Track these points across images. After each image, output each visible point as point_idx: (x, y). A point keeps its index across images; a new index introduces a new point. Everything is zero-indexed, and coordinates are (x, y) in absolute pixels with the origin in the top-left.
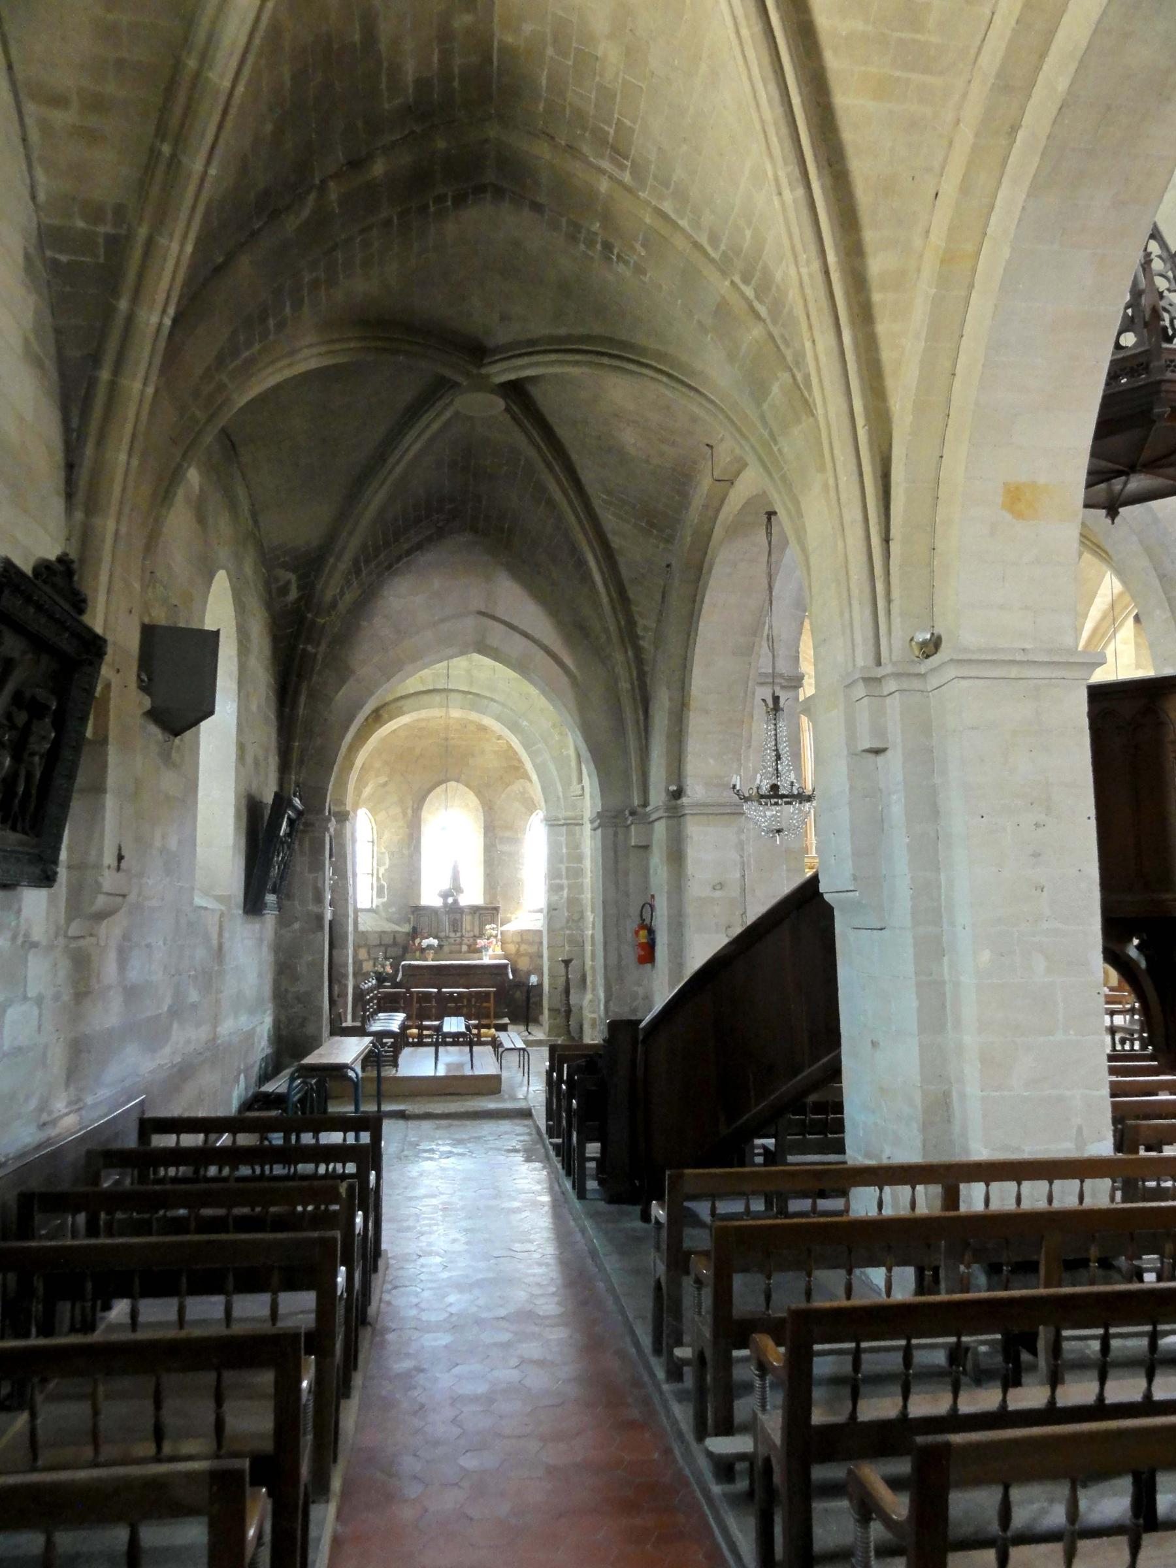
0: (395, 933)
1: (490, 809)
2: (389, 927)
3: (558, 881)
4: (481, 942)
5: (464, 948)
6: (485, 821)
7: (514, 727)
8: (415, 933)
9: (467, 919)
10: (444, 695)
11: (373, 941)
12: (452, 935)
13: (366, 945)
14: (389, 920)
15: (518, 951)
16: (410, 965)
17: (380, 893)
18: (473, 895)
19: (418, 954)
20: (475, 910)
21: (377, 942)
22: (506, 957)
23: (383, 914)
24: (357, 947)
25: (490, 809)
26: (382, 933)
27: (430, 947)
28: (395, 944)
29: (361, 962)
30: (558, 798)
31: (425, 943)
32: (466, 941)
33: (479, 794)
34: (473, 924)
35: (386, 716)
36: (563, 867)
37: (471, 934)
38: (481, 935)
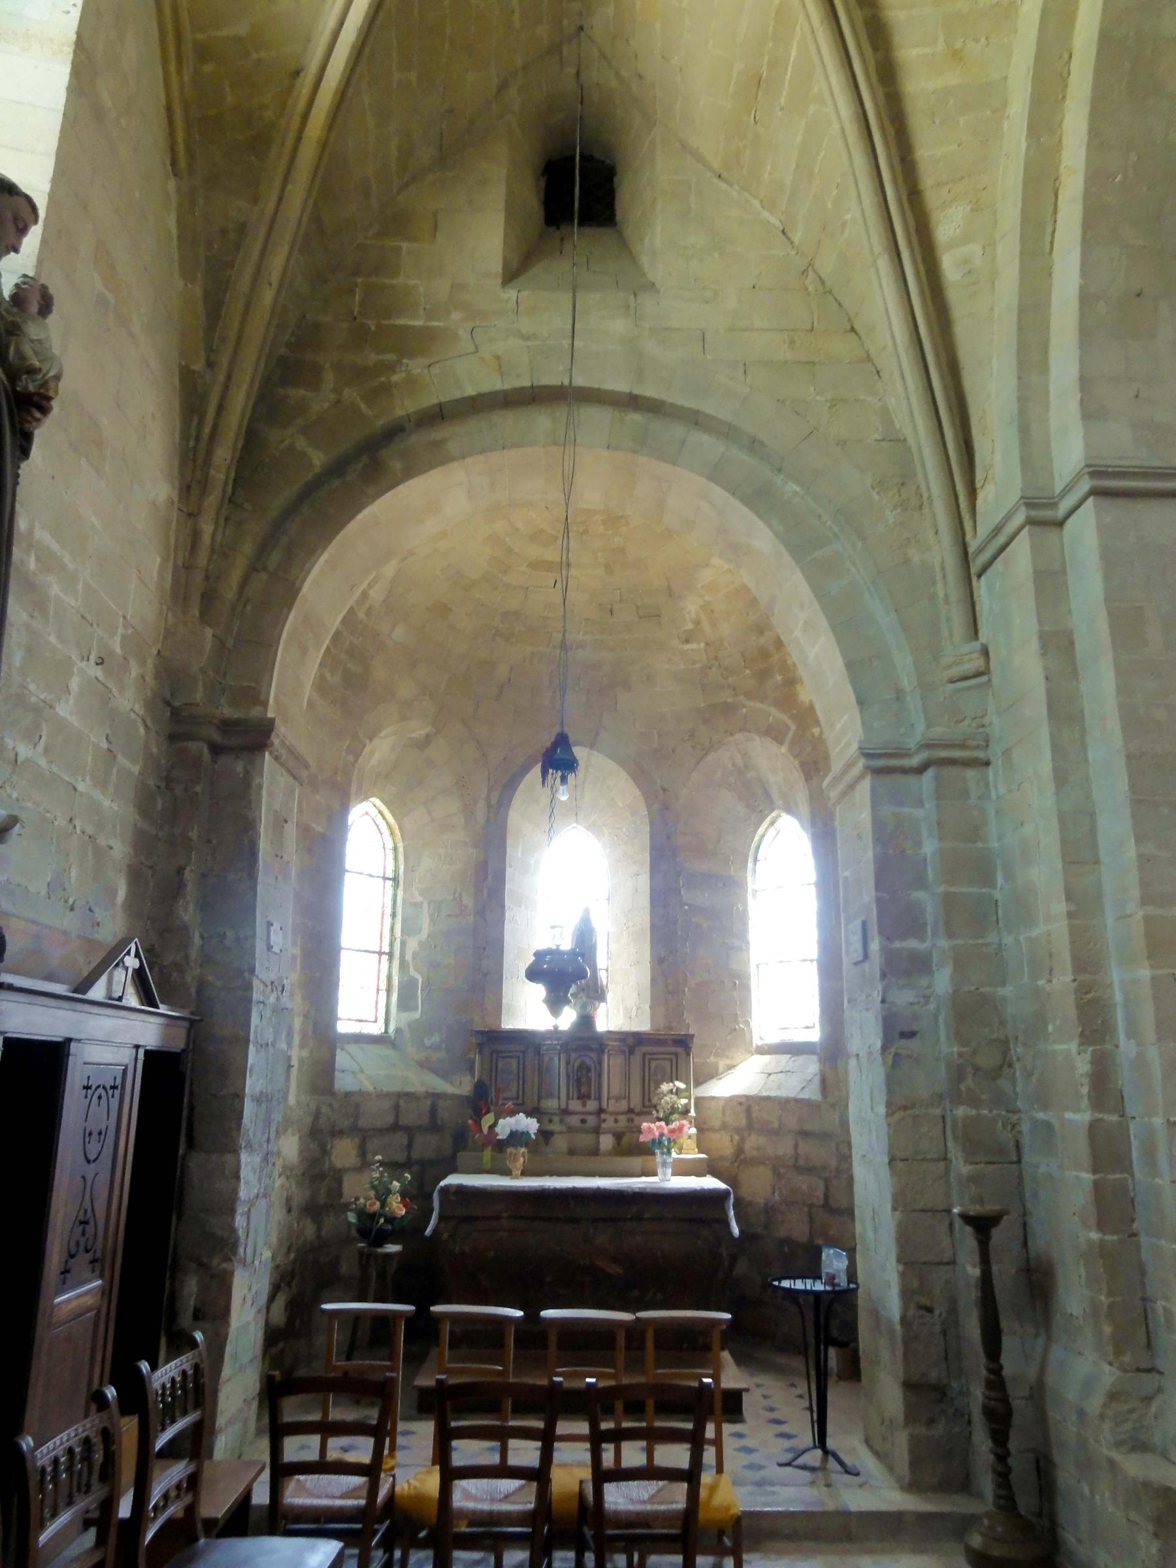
0: (436, 1096)
1: (666, 807)
3: (912, 944)
4: (651, 1129)
5: (606, 1142)
6: (653, 837)
7: (759, 499)
8: (480, 1101)
9: (612, 1065)
10: (561, 412)
11: (377, 1115)
12: (575, 1105)
13: (354, 1129)
14: (424, 1064)
15: (740, 1151)
16: (461, 1190)
17: (405, 1003)
18: (620, 1011)
19: (488, 1154)
20: (631, 1042)
21: (390, 1119)
23: (411, 1050)
24: (319, 1135)
25: (666, 807)
26: (400, 1099)
27: (516, 1138)
28: (434, 1126)
29: (337, 1176)
30: (899, 695)
31: (506, 1126)
32: (609, 1123)
33: (639, 774)
34: (627, 1077)
35: (397, 465)
36: (928, 901)
38: (648, 1108)
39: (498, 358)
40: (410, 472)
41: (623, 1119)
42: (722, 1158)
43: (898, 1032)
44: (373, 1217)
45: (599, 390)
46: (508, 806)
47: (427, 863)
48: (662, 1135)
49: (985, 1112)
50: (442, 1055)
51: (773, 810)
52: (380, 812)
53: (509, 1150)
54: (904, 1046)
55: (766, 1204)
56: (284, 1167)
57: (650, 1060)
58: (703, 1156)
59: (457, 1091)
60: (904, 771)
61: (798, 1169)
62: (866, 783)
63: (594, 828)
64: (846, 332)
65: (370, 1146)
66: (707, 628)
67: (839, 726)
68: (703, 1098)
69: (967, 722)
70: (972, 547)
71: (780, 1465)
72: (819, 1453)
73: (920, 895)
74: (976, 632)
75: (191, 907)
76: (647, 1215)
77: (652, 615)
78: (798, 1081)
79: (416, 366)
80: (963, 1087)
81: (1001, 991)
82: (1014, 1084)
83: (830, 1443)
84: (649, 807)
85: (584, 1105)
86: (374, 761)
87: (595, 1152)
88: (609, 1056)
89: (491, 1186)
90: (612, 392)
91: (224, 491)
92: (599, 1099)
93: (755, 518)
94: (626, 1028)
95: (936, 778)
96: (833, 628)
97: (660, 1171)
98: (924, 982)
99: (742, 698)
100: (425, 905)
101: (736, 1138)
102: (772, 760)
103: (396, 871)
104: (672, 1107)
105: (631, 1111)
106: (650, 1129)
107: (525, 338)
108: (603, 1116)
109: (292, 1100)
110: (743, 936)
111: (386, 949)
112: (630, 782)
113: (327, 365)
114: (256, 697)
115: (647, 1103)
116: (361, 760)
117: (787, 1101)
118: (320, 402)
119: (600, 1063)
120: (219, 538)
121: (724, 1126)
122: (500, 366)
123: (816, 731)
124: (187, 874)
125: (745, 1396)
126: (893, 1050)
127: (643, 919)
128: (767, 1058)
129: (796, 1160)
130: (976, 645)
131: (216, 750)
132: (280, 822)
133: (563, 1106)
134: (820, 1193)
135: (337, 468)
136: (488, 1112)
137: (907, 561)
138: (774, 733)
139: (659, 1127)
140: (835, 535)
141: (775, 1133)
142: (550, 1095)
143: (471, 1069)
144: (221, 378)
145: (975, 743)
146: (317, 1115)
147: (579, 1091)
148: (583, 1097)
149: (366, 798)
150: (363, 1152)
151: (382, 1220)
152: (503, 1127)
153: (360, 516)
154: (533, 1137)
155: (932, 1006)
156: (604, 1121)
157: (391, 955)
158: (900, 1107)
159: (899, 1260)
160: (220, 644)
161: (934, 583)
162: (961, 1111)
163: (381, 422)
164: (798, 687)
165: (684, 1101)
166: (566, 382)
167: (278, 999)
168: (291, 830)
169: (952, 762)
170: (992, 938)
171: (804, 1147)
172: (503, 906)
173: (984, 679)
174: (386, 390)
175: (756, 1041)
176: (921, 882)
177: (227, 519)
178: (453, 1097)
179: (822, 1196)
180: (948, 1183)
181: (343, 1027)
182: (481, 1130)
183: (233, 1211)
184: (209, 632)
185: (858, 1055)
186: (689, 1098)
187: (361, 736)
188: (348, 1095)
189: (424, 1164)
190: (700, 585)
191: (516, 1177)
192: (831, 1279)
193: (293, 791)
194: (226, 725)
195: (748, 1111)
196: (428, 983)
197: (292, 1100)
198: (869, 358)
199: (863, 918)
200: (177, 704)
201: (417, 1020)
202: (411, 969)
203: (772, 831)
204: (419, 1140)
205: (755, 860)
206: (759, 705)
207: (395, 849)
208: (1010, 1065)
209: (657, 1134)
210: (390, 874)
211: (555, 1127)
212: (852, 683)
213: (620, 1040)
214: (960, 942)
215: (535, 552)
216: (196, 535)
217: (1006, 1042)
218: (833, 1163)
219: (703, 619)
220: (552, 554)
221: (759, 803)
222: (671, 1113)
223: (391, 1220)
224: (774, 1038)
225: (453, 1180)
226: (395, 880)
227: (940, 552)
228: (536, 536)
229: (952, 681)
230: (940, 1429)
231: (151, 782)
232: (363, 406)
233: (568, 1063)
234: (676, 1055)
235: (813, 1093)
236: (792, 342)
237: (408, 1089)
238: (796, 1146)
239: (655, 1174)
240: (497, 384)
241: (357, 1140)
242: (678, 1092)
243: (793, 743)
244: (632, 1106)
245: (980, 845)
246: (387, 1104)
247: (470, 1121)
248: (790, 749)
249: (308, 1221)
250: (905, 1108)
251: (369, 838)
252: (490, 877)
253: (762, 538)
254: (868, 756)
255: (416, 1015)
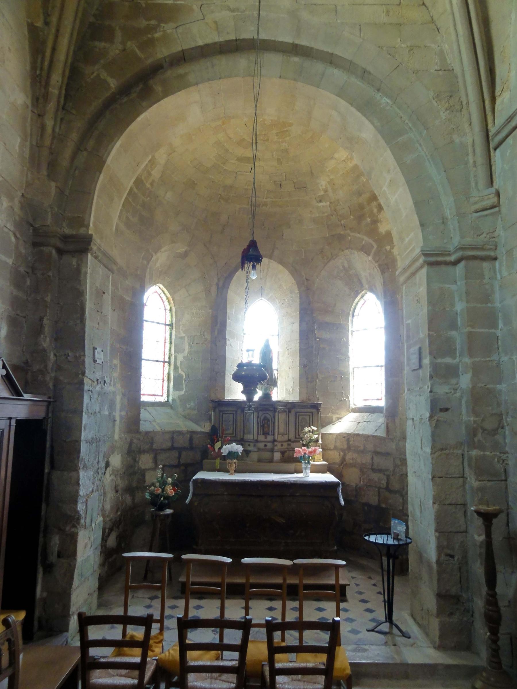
0: (193, 433)
1: (308, 289)
2: (185, 426)
3: (448, 360)
4: (300, 451)
5: (277, 456)
6: (301, 304)
7: (366, 107)
8: (214, 435)
9: (280, 418)
12: (262, 438)
13: (151, 450)
15: (343, 460)
16: (204, 481)
17: (177, 386)
18: (284, 390)
19: (218, 461)
20: (289, 407)
21: (169, 444)
22: (329, 469)
23: (180, 410)
24: (132, 453)
26: (174, 434)
27: (232, 455)
28: (191, 447)
29: (143, 473)
30: (444, 221)
31: (226, 449)
32: (278, 447)
33: (295, 272)
34: (287, 423)
35: (159, 89)
37: (286, 438)
39: (216, 22)
40: (166, 94)
41: (285, 444)
42: (334, 463)
43: (439, 408)
44: (158, 496)
45: (274, 41)
46: (228, 288)
47: (187, 317)
48: (305, 454)
49: (488, 453)
50: (195, 412)
51: (363, 290)
52: (163, 291)
53: (228, 461)
54: (443, 416)
55: (356, 486)
56: (113, 471)
57: (299, 415)
58: (325, 463)
59: (203, 430)
60: (446, 263)
61: (374, 470)
62: (424, 270)
63: (272, 300)
64: (419, 5)
65: (159, 457)
66: (330, 193)
67: (407, 240)
68: (325, 434)
69: (484, 235)
70: (492, 130)
71: (368, 631)
72: (388, 624)
73: (454, 333)
74: (492, 182)
75: (48, 339)
76: (298, 494)
77: (301, 187)
78: (375, 426)
79: (168, 28)
80: (476, 439)
81: (498, 387)
82: (505, 438)
83: (394, 618)
84: (299, 289)
85: (266, 438)
86: (158, 265)
87: (271, 461)
88: (279, 413)
89: (219, 479)
90: (282, 43)
91: (58, 101)
92: (274, 435)
93: (364, 119)
94: (287, 399)
95: (466, 267)
96: (407, 182)
97: (304, 471)
98: (454, 381)
99: (349, 231)
100: (186, 338)
101: (342, 453)
102: (363, 264)
103: (171, 321)
104: (310, 439)
105: (289, 440)
106: (299, 452)
107: (232, 11)
108: (275, 443)
109: (116, 437)
110: (347, 355)
111: (167, 359)
112: (290, 276)
113: (117, 28)
114: (82, 222)
115: (297, 437)
116: (151, 263)
117: (368, 436)
118: (114, 50)
119: (274, 417)
120: (57, 130)
121: (336, 448)
122: (217, 28)
123: (388, 248)
124: (46, 321)
125: (347, 587)
126: (436, 418)
127: (296, 345)
128: (356, 415)
129: (372, 465)
130: (493, 190)
131: (60, 252)
132: (100, 293)
133: (256, 438)
134: (384, 482)
135: (125, 90)
136: (218, 441)
137: (452, 142)
138: (365, 250)
139: (304, 450)
140: (410, 128)
141: (363, 452)
142: (249, 433)
143: (210, 419)
144: (53, 31)
145: (489, 247)
146: (131, 443)
147: (263, 430)
148: (265, 434)
149: (155, 284)
150: (155, 461)
151: (162, 499)
152: (225, 449)
153: (139, 119)
154: (240, 454)
155: (458, 395)
156: (276, 445)
157: (169, 363)
158: (439, 449)
159: (436, 531)
160: (61, 192)
161: (468, 155)
162: (475, 453)
163: (150, 61)
164: (379, 224)
165: (317, 436)
166: (256, 37)
167: (102, 388)
168: (107, 298)
169: (475, 258)
170: (495, 357)
171: (377, 459)
172: (226, 339)
173: (497, 209)
174: (151, 42)
175: (352, 406)
176: (453, 326)
177: (62, 119)
178: (201, 433)
179: (385, 484)
180: (464, 490)
181: (143, 399)
182: (214, 450)
183: (76, 502)
184: (53, 184)
185: (413, 419)
186: (318, 434)
187: (150, 251)
188: (147, 433)
189: (187, 465)
190: (328, 170)
191: (231, 474)
192: (396, 537)
193: (108, 277)
194: (65, 238)
195: (348, 441)
196: (188, 376)
197: (116, 437)
198: (433, 21)
199: (420, 346)
200: (37, 226)
201: (183, 395)
202: (180, 369)
203: (362, 301)
204: (184, 454)
205: (353, 316)
206: (358, 235)
207: (171, 310)
208: (503, 428)
209: (303, 453)
210: (168, 322)
211: (251, 448)
212: (417, 214)
213: (286, 406)
214: (476, 359)
215: (240, 152)
216: (43, 127)
217: (501, 415)
218: (391, 469)
219: (329, 189)
220: (249, 154)
221: (356, 287)
222: (309, 442)
223: (167, 498)
224: (361, 404)
225: (200, 475)
226: (171, 325)
227: (473, 136)
228: (240, 143)
229: (477, 212)
230: (455, 619)
231: (22, 269)
232: (138, 51)
233: (258, 417)
234: (312, 413)
235: (382, 433)
236: (388, 11)
237: (178, 430)
238: (372, 458)
239: (301, 472)
240: (214, 38)
241: (152, 455)
242: (313, 432)
243: (375, 254)
244: (290, 438)
245: (489, 305)
246: (167, 436)
247: (209, 446)
248: (374, 258)
249: (128, 496)
250: (442, 449)
251: (156, 305)
252: (218, 325)
253: (368, 131)
254: (425, 255)
255: (182, 393)
